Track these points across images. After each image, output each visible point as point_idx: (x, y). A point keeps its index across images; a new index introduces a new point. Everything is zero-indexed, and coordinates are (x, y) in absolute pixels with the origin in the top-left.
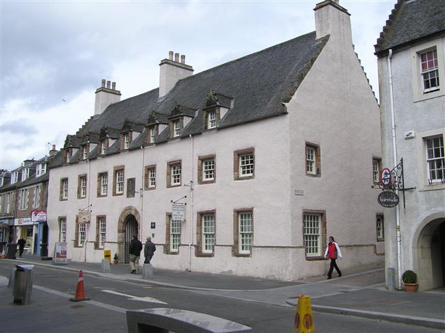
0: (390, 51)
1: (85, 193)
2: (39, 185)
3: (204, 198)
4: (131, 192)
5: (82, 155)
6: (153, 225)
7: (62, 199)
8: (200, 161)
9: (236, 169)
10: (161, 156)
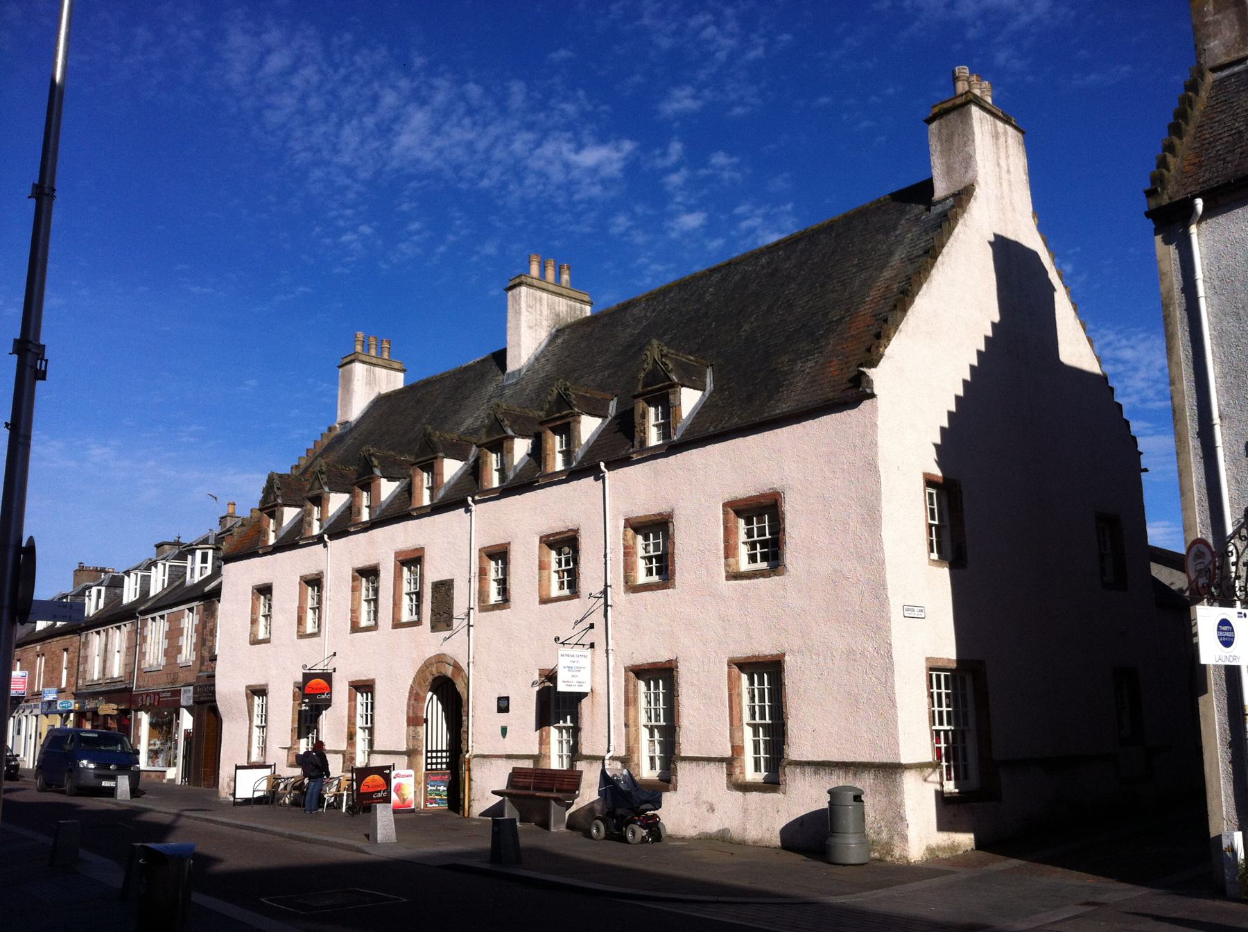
0: (1199, 203)
2: (194, 604)
4: (443, 618)
6: (503, 704)
9: (730, 551)
10: (523, 520)
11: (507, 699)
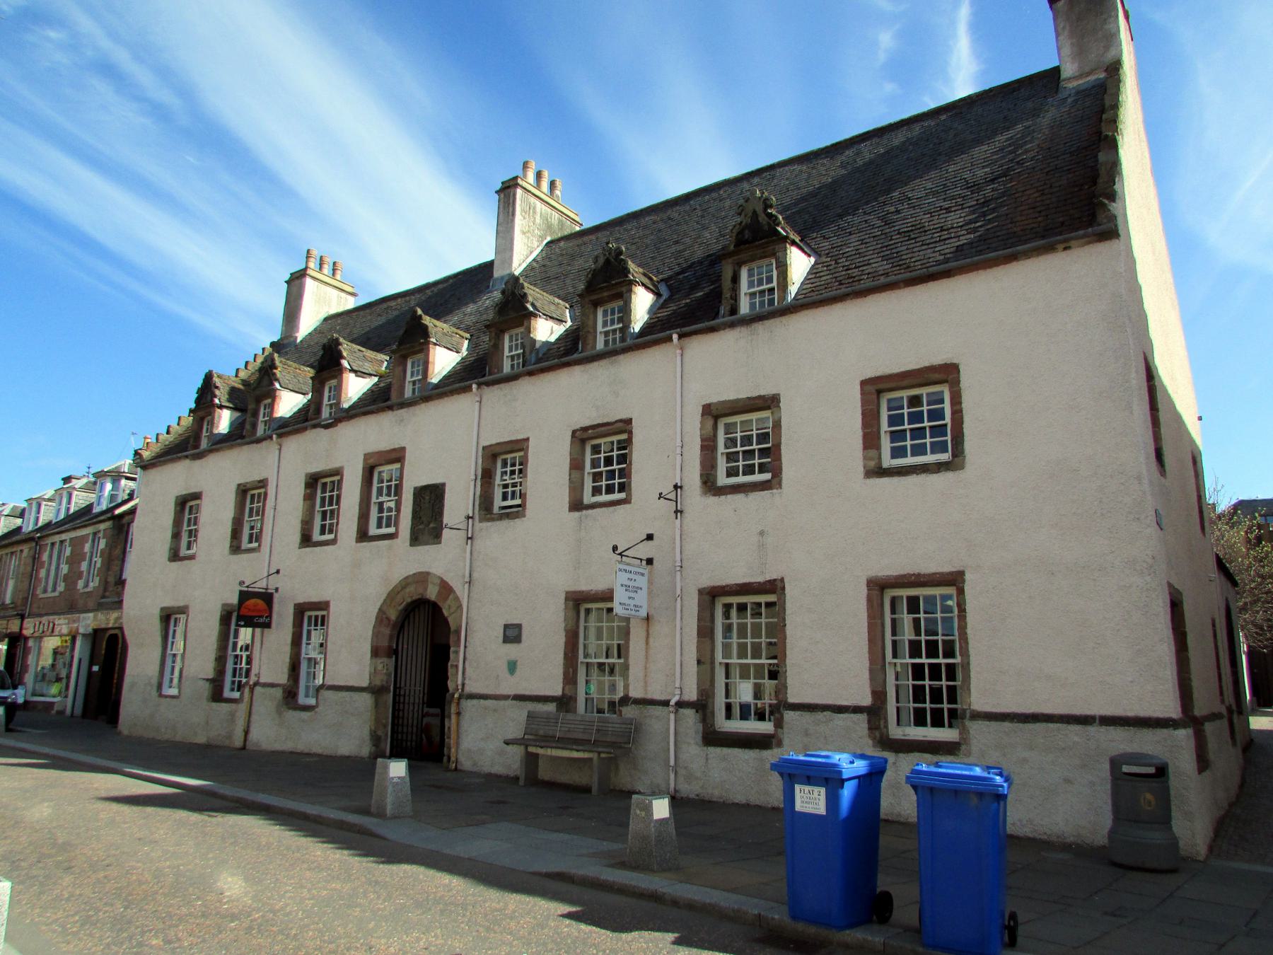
1: (256, 537)
2: (102, 526)
3: (728, 538)
5: (254, 426)
6: (510, 633)
7: (175, 556)
8: (710, 423)
9: (870, 441)
11: (519, 626)
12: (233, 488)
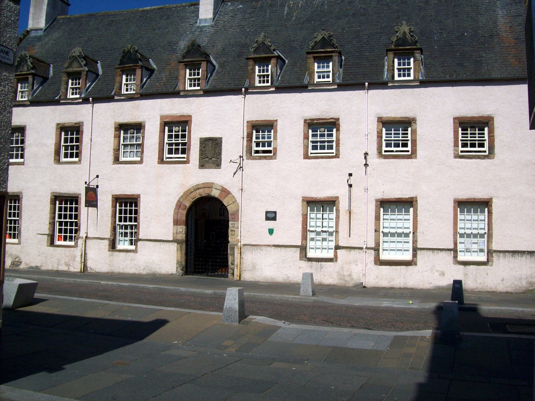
6: (269, 215)
12: (54, 126)
